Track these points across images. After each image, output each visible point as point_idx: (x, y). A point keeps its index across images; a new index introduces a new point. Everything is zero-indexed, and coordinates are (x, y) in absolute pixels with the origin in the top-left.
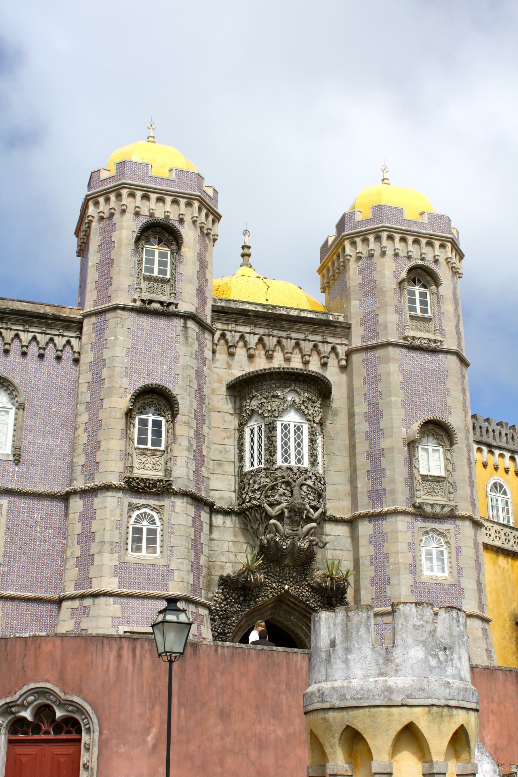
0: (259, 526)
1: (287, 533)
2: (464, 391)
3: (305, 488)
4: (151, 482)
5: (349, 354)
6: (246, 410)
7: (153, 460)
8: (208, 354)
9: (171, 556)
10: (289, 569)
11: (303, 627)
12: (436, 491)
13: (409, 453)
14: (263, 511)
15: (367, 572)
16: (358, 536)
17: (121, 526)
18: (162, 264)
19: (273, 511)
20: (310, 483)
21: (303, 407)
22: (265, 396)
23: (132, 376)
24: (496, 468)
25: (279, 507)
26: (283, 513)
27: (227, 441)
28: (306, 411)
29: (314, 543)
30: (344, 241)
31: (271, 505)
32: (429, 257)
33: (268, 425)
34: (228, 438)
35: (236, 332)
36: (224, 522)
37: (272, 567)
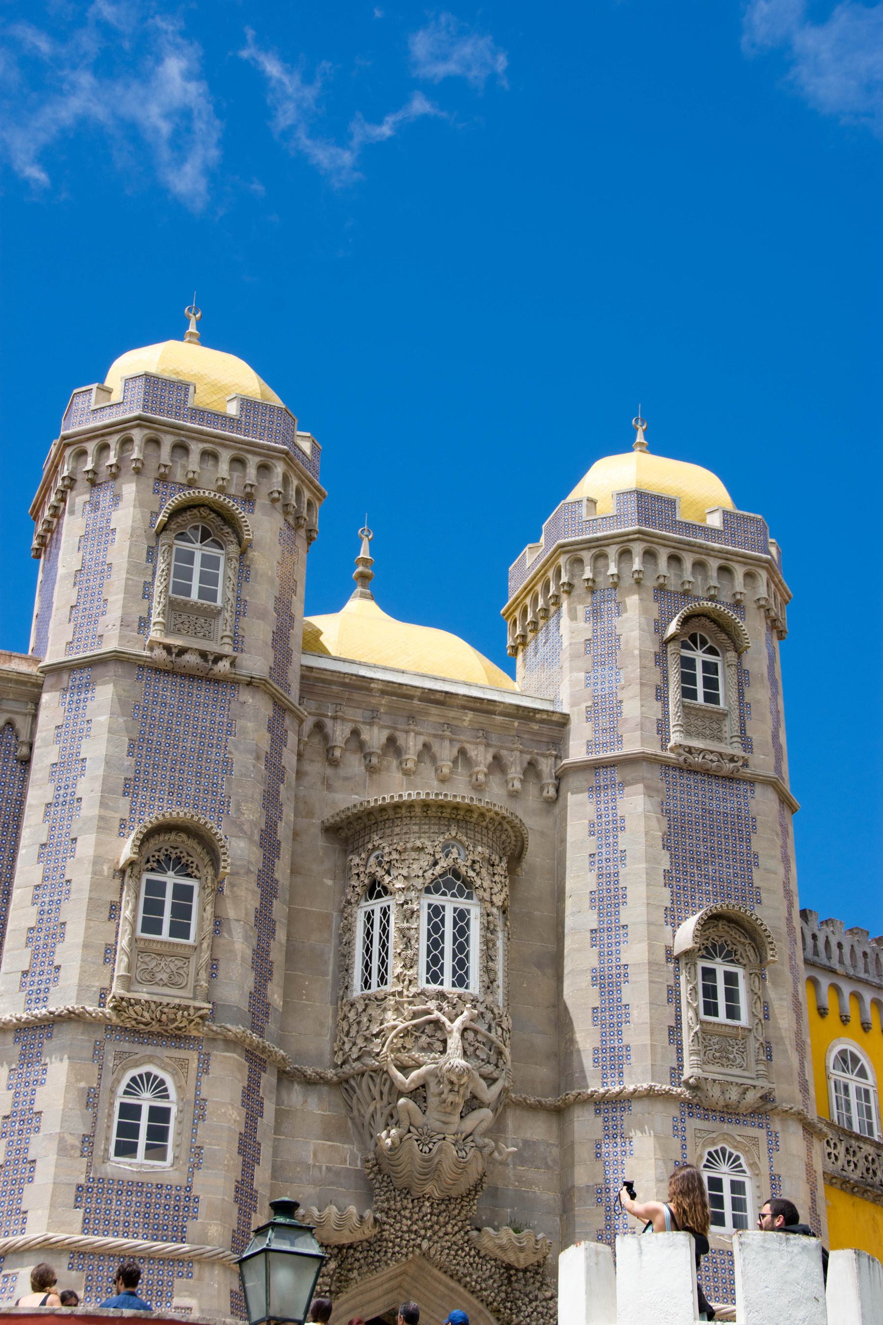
2: (786, 859)
3: (470, 1035)
6: (358, 875)
7: (172, 965)
8: (289, 759)
9: (196, 1166)
10: (432, 1205)
12: (731, 1056)
14: (386, 1080)
16: (573, 1143)
17: (96, 1100)
18: (208, 579)
19: (406, 1081)
21: (471, 873)
22: (399, 848)
23: (138, 794)
24: (845, 1020)
28: (478, 882)
30: (559, 555)
32: (726, 597)
33: (402, 905)
37: (398, 1199)
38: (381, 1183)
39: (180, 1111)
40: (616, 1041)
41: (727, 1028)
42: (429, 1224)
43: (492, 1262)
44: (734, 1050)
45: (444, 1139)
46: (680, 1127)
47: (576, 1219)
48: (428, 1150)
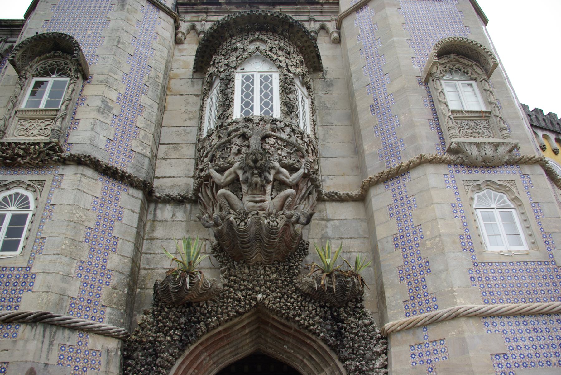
0: (213, 210)
1: (248, 208)
3: (271, 141)
4: (23, 147)
5: (339, 27)
10: (264, 269)
11: (305, 360)
12: (480, 131)
13: (429, 92)
15: (392, 260)
16: (373, 213)
20: (284, 136)
22: (223, 53)
25: (231, 169)
26: (237, 178)
27: (188, 123)
28: (275, 57)
29: (294, 219)
31: (221, 171)
34: (190, 119)
35: (206, 21)
36: (174, 215)
37: (236, 267)
38: (222, 258)
39: (34, 215)
40: (393, 140)
41: (473, 114)
42: (262, 282)
43: (317, 304)
44: (482, 127)
45: (257, 214)
46: (450, 181)
47: (381, 263)
48: (243, 223)
